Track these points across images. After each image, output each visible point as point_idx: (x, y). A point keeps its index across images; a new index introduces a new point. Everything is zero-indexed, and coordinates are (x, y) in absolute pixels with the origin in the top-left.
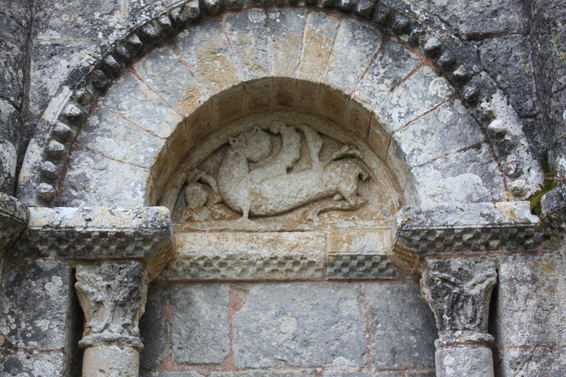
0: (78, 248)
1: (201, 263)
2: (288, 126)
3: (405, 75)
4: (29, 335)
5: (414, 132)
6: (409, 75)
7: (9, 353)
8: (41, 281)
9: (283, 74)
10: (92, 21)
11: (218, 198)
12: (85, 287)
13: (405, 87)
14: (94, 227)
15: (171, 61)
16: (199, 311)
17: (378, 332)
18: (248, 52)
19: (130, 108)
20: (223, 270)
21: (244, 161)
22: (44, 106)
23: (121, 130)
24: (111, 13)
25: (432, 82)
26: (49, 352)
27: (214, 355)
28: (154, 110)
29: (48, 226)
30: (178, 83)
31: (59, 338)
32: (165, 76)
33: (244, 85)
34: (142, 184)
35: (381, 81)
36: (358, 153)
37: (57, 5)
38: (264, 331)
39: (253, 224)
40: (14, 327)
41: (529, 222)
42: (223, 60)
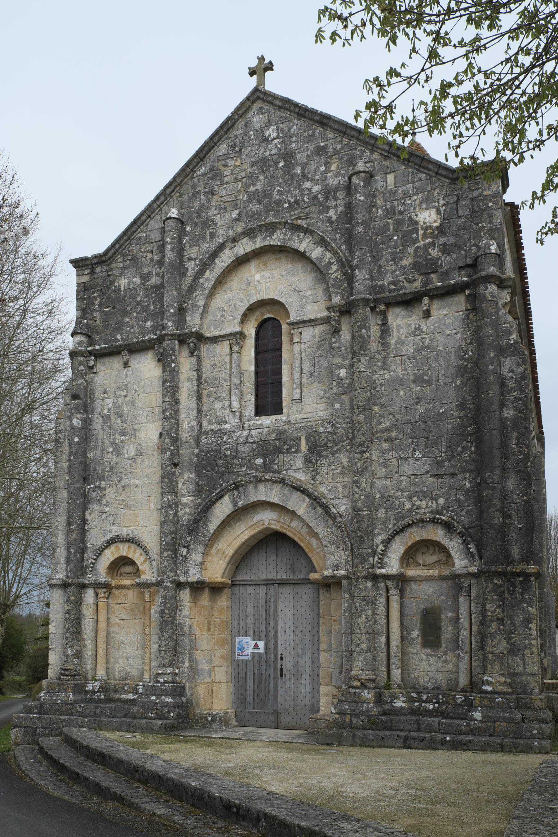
0: (386, 577)
22: (377, 547)
27: (416, 595)
31: (384, 594)
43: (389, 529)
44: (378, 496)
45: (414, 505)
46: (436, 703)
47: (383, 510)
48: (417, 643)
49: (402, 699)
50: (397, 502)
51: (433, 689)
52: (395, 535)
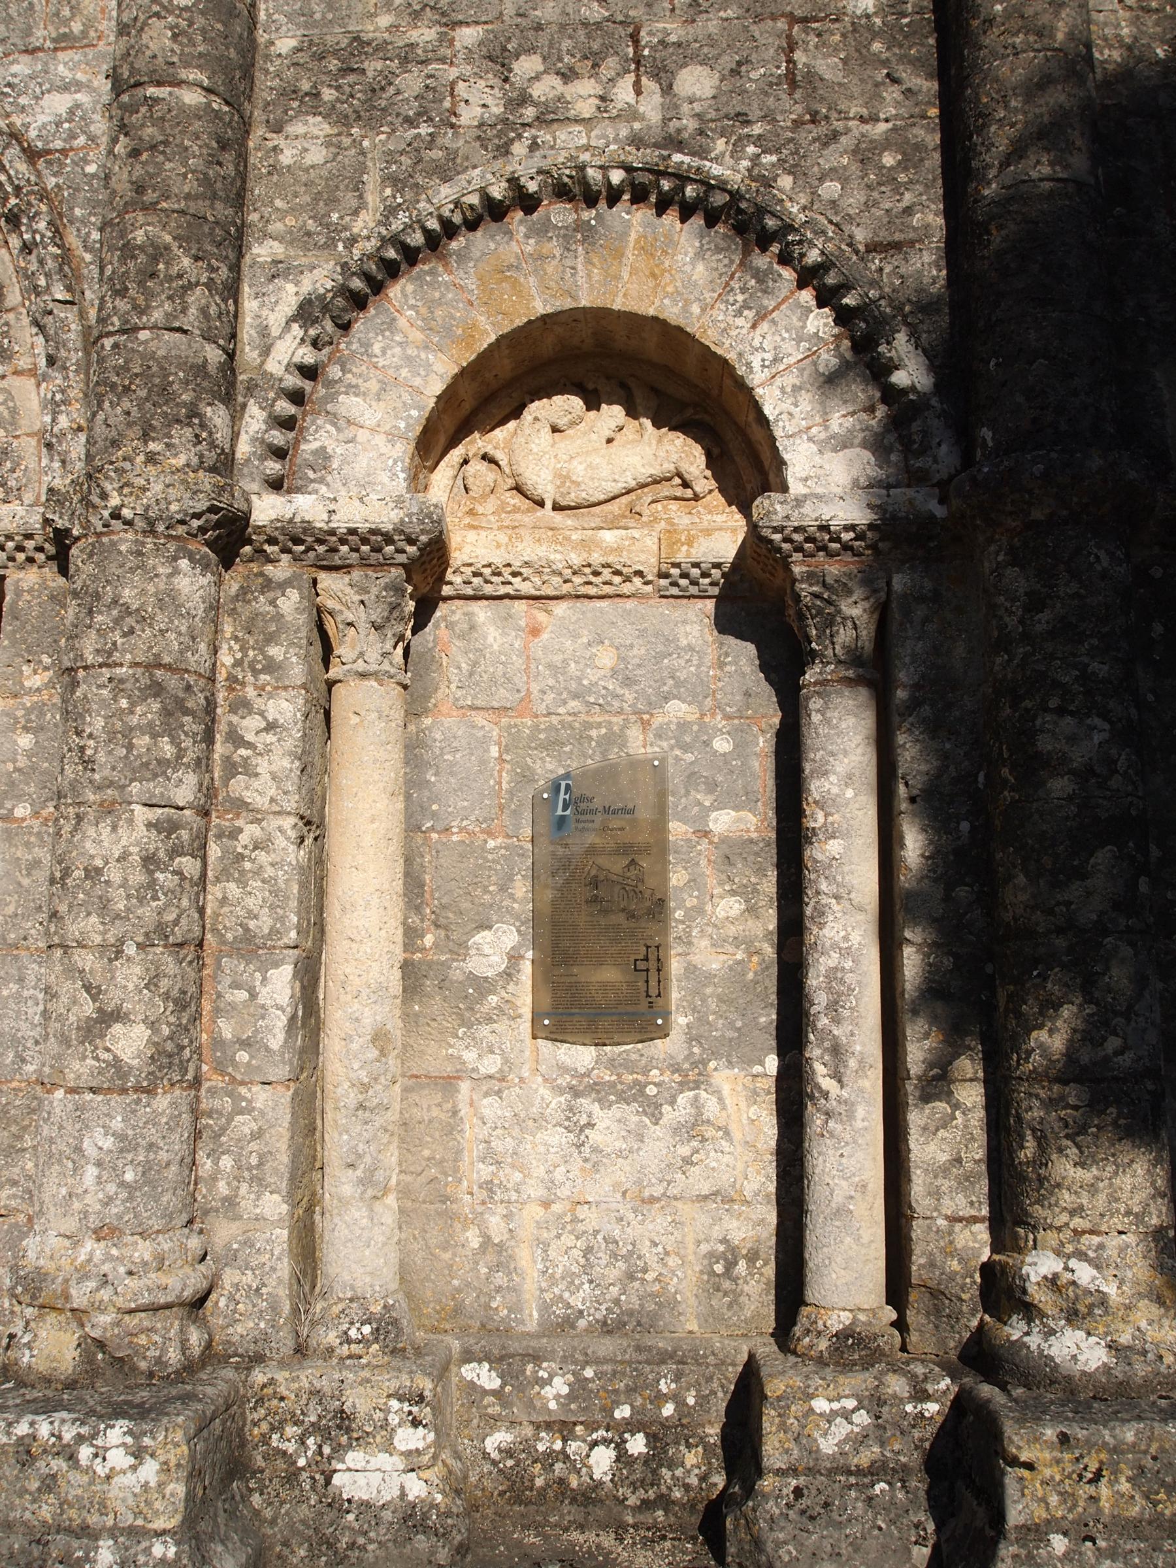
1: (487, 571)
2: (608, 378)
3: (773, 304)
4: (259, 667)
5: (782, 389)
6: (780, 304)
7: (233, 689)
8: (271, 595)
9: (599, 303)
10: (328, 226)
11: (510, 482)
12: (330, 604)
13: (773, 321)
14: (341, 523)
15: (440, 284)
16: (485, 638)
17: (727, 668)
18: (550, 270)
19: (384, 353)
20: (517, 581)
21: (548, 429)
22: (266, 351)
23: (373, 385)
24: (356, 213)
25: (812, 316)
26: (285, 688)
27: (503, 696)
28: (418, 356)
29: (278, 520)
30: (453, 317)
32: (432, 305)
33: (544, 318)
34: (403, 462)
35: (739, 313)
36: (707, 418)
37: (279, 203)
38: (573, 665)
39: (558, 517)
40: (239, 655)
41: (932, 516)
42: (515, 283)
43: (353, 241)
44: (285, 45)
45: (524, 99)
46: (631, 1425)
47: (317, 126)
48: (506, 1011)
49: (410, 1439)
50: (411, 82)
51: (606, 1328)
52: (392, 270)
